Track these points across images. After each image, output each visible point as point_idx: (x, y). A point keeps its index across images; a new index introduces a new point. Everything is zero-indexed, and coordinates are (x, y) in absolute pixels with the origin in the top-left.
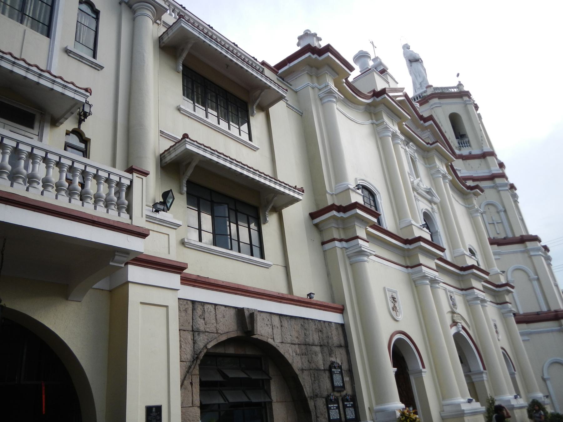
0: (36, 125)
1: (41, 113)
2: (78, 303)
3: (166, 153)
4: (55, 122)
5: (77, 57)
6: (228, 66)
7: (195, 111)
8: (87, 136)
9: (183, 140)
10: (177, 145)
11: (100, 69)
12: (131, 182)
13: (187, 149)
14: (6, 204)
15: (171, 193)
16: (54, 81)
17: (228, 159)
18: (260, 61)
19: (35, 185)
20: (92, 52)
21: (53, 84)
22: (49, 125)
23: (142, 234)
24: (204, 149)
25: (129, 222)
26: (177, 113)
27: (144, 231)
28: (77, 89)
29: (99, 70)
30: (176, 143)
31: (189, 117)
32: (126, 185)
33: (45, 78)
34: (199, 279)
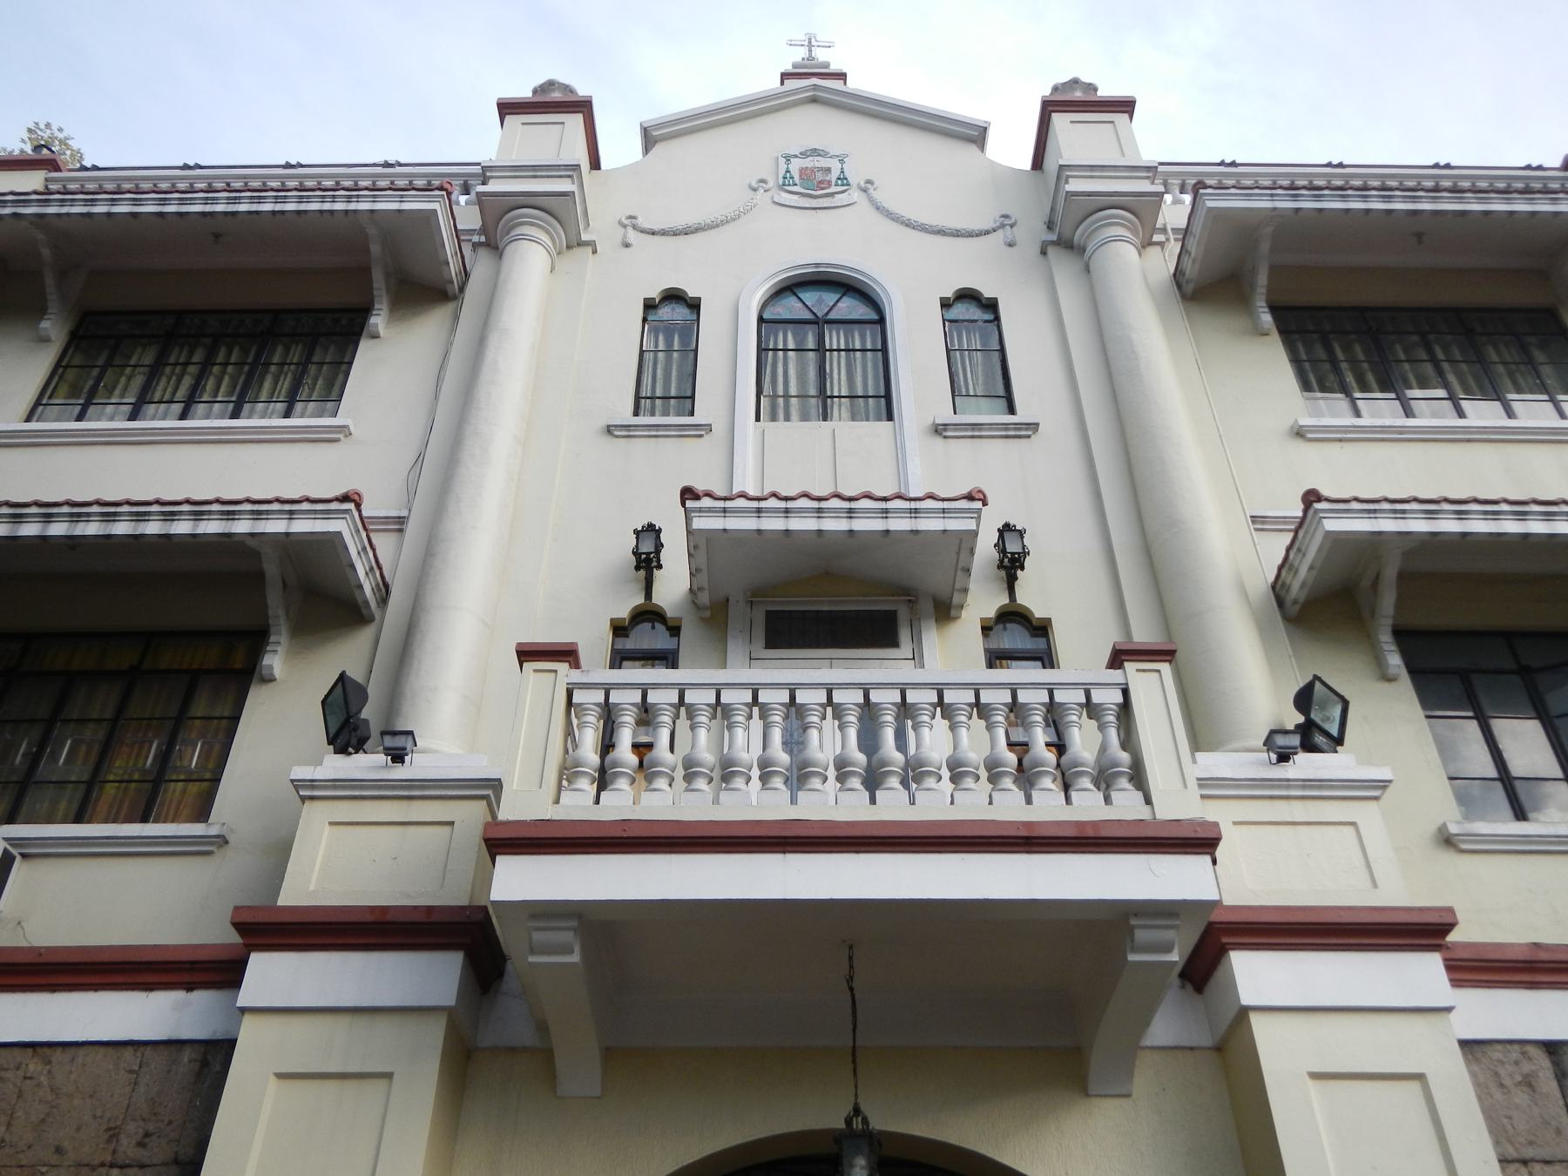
0: (904, 635)
1: (910, 601)
2: (1123, 1101)
3: (1284, 573)
4: (945, 611)
6: (1419, 236)
7: (1358, 414)
8: (1039, 612)
9: (1311, 512)
10: (1301, 534)
11: (1030, 433)
12: (1126, 692)
13: (1328, 533)
14: (784, 852)
15: (1318, 685)
16: (886, 511)
17: (1505, 507)
18: (1558, 163)
19: (930, 782)
20: (1002, 403)
21: (886, 517)
22: (933, 623)
23: (1202, 842)
24: (1395, 511)
25: (1143, 813)
26: (1301, 445)
27: (1198, 829)
28: (946, 505)
29: (1029, 437)
30: (1296, 532)
31: (1340, 440)
32: (1038, 706)
34: (1544, 956)
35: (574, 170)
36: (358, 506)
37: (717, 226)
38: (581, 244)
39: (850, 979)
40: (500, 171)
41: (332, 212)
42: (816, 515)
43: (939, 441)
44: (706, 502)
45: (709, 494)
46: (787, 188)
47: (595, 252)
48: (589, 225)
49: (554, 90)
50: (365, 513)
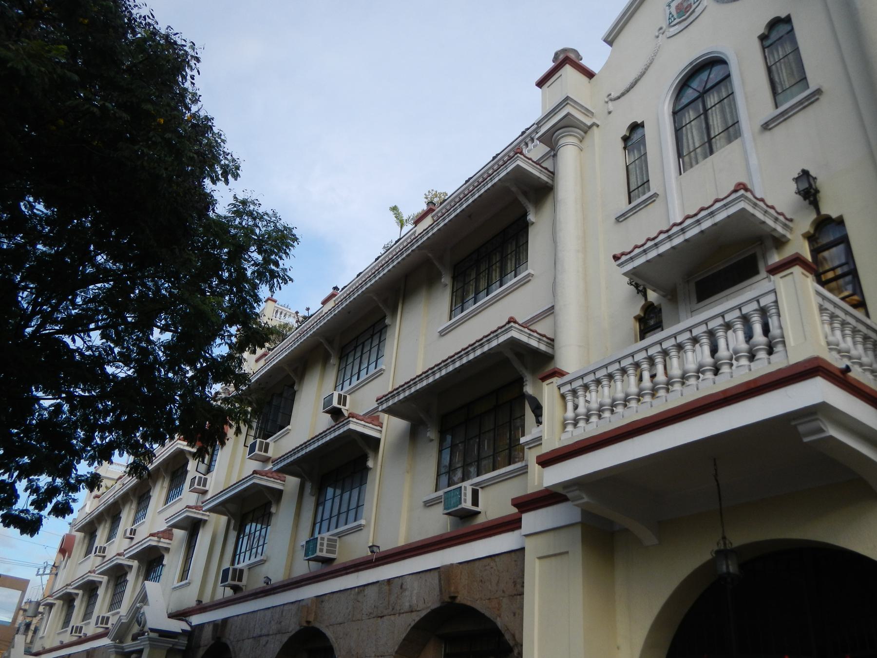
5: (778, 119)
8: (834, 215)
22: (774, 251)
33: (689, 227)
35: (567, 100)
36: (515, 322)
37: (644, 73)
38: (590, 127)
39: (716, 476)
40: (542, 121)
41: (489, 189)
42: (669, 240)
43: (768, 134)
44: (624, 258)
45: (623, 254)
46: (672, 24)
47: (598, 126)
48: (593, 113)
49: (559, 56)
50: (520, 322)
